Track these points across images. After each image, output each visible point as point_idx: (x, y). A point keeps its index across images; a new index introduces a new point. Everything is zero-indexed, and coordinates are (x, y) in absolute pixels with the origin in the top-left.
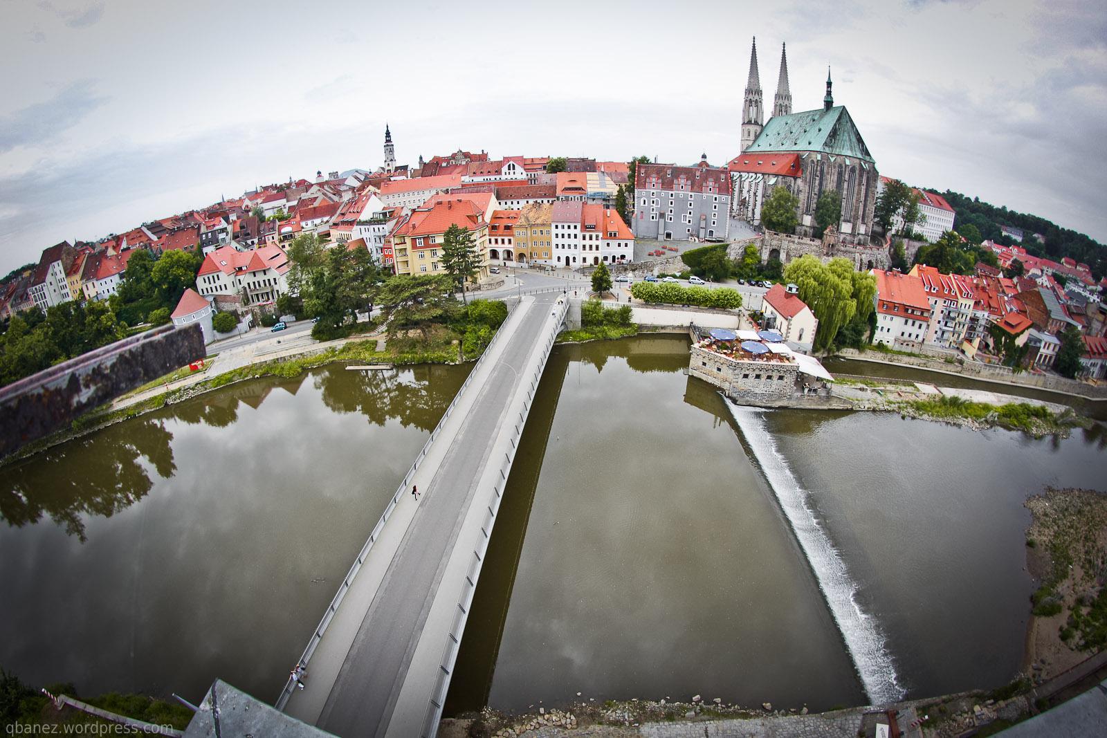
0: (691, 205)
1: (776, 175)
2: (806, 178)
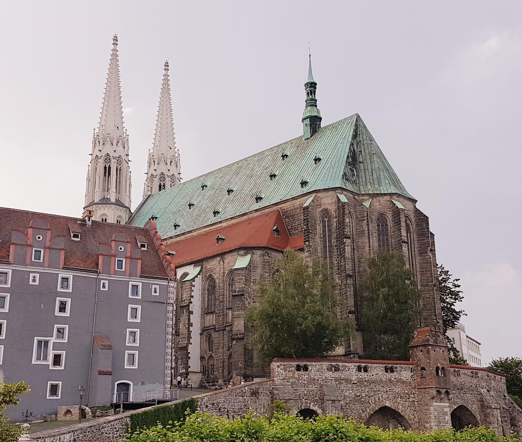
0: (62, 308)
1: (247, 249)
2: (316, 250)
